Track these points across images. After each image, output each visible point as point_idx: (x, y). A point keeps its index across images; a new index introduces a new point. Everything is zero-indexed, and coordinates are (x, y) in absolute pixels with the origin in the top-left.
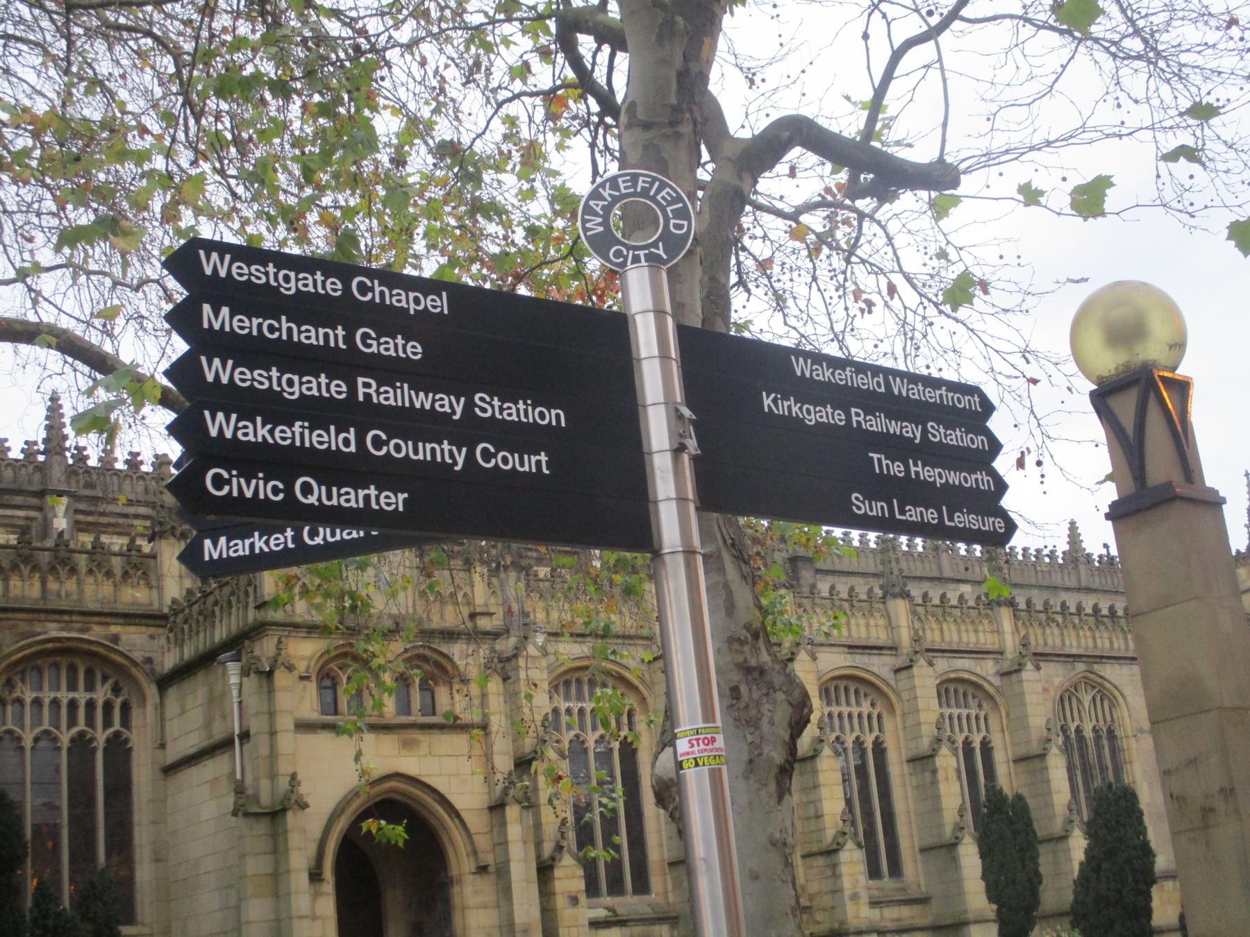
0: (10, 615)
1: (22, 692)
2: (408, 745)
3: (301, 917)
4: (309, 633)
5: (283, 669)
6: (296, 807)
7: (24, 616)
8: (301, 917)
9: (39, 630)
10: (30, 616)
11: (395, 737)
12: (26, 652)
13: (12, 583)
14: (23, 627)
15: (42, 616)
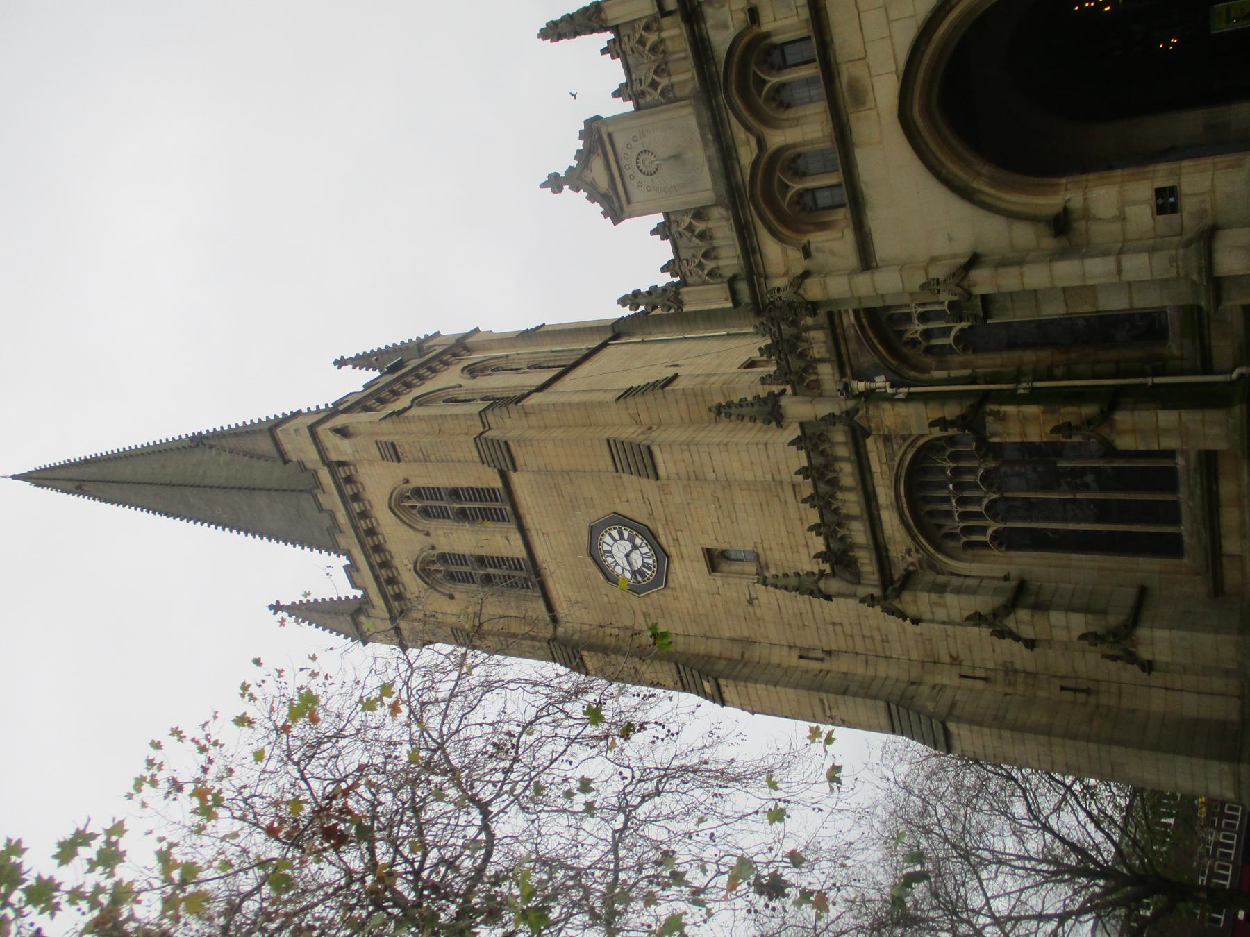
0: (845, 358)
1: (916, 332)
2: (859, 96)
3: (1119, 271)
4: (754, 252)
5: (801, 291)
6: (965, 284)
7: (843, 348)
8: (1119, 271)
9: (853, 332)
10: (842, 342)
11: (853, 117)
12: (875, 341)
13: (817, 356)
14: (853, 346)
15: (839, 331)
